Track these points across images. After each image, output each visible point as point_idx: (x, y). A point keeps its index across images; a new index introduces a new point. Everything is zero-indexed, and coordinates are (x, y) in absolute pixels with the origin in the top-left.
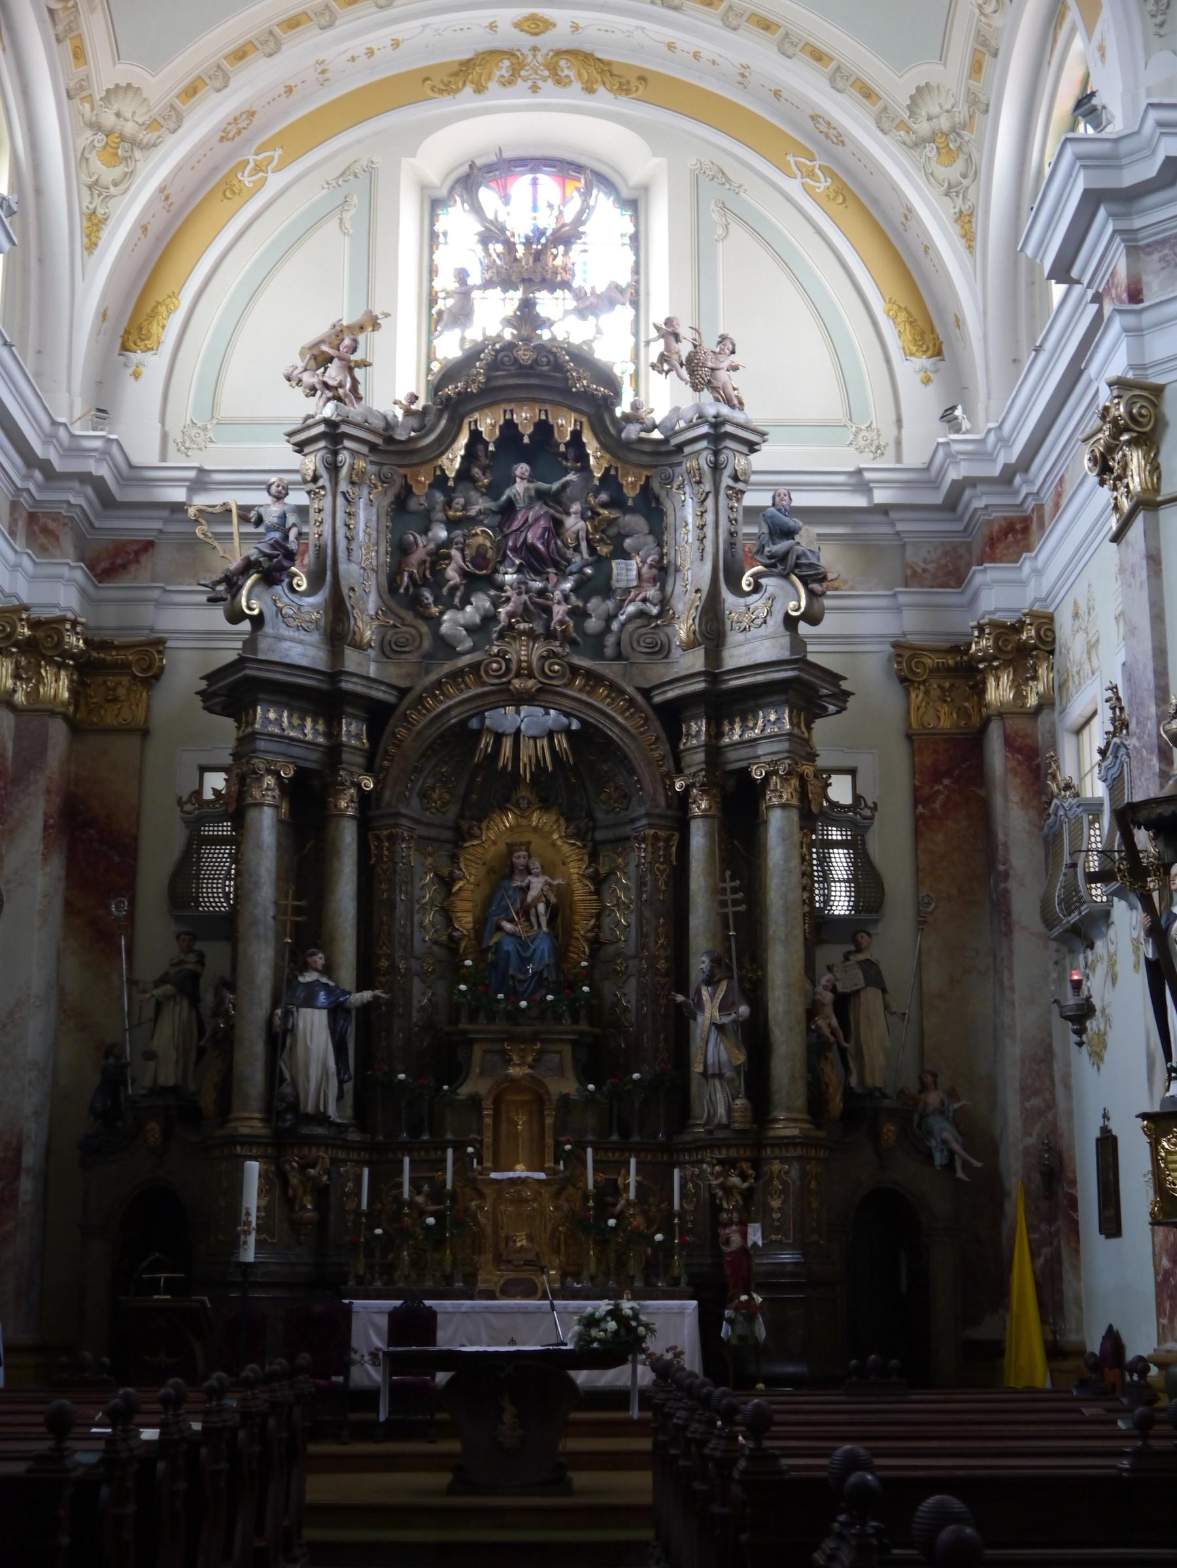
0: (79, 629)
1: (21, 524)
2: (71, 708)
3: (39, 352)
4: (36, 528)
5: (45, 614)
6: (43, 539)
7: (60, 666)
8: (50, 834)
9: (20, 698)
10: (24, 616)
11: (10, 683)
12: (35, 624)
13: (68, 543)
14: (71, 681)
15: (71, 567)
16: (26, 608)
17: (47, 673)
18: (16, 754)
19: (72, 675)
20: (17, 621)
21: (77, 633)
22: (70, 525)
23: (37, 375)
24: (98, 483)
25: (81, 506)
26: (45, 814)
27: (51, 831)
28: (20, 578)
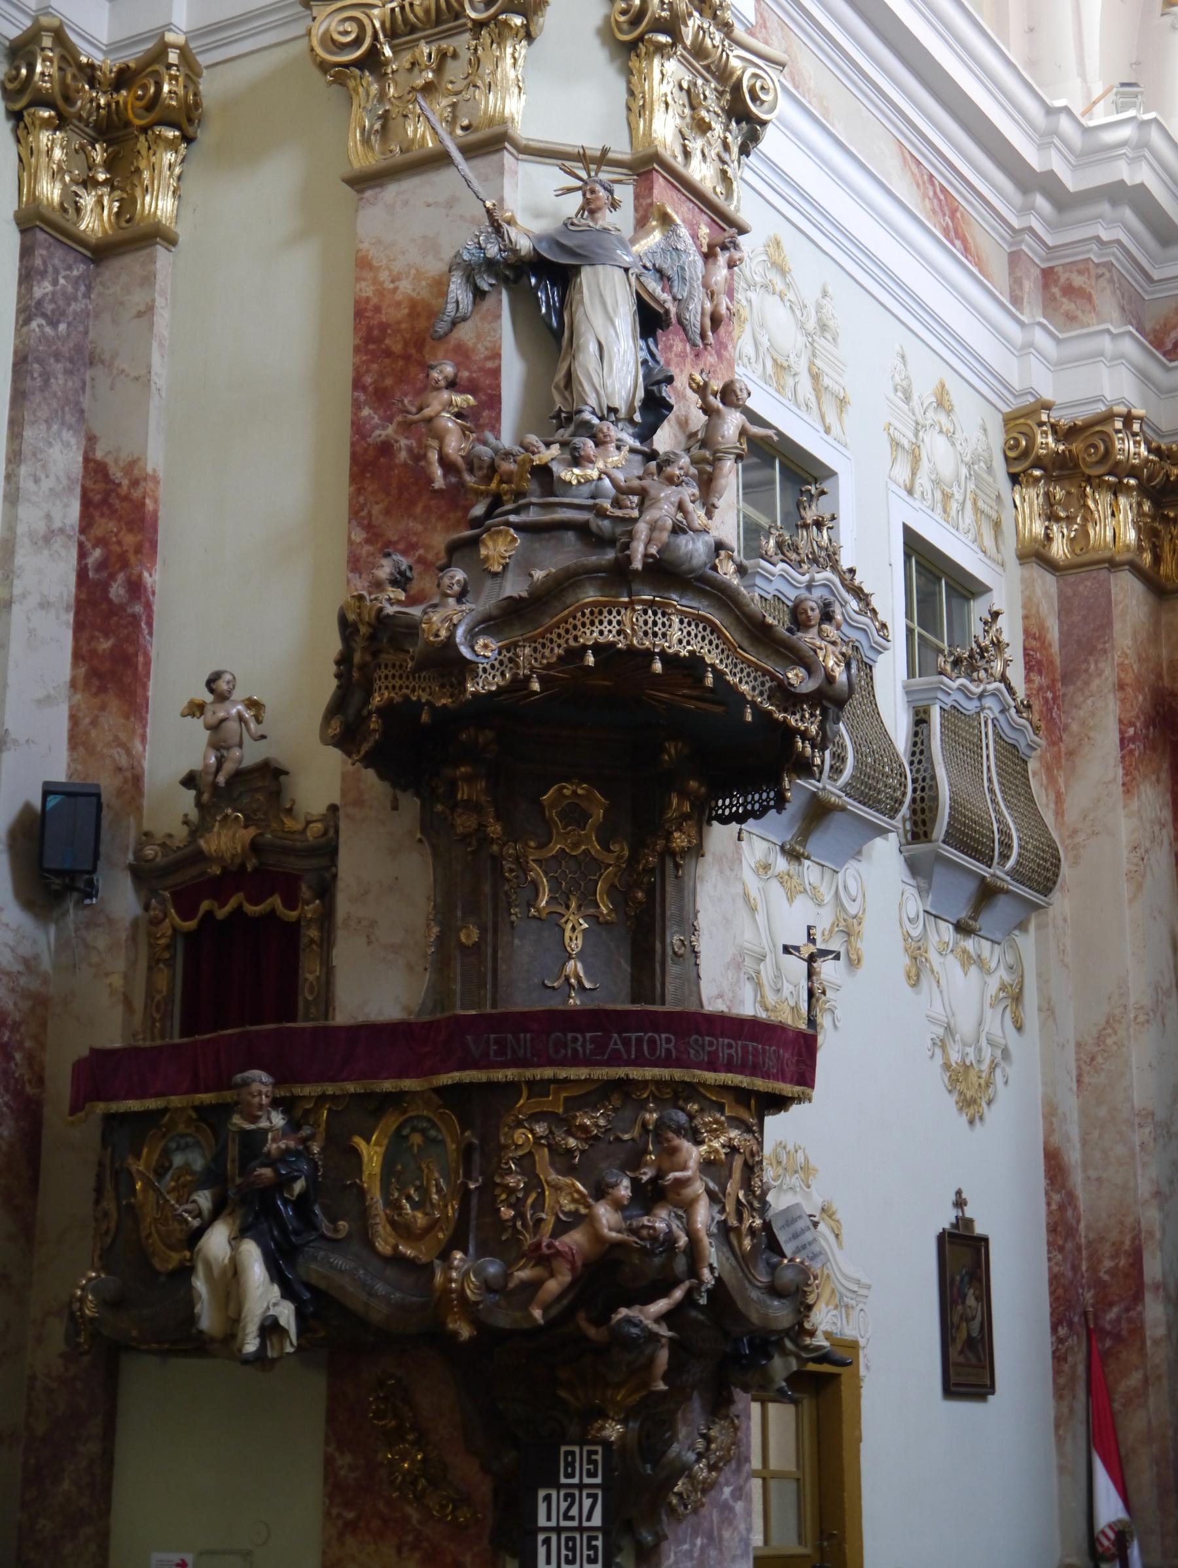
0: (1136, 427)
1: (1030, 286)
2: (1147, 557)
3: (1031, 30)
4: (1056, 290)
5: (1081, 415)
6: (1067, 305)
7: (1117, 490)
8: (1131, 752)
9: (1059, 549)
10: (1044, 418)
11: (1038, 528)
12: (1068, 433)
13: (1107, 302)
14: (1140, 514)
15: (1114, 337)
16: (1047, 407)
17: (1099, 502)
18: (1065, 637)
19: (1140, 505)
20: (1035, 428)
21: (1135, 435)
22: (1108, 275)
23: (1032, 64)
24: (1138, 198)
25: (1119, 242)
26: (1120, 721)
27: (1132, 746)
28: (1034, 363)
